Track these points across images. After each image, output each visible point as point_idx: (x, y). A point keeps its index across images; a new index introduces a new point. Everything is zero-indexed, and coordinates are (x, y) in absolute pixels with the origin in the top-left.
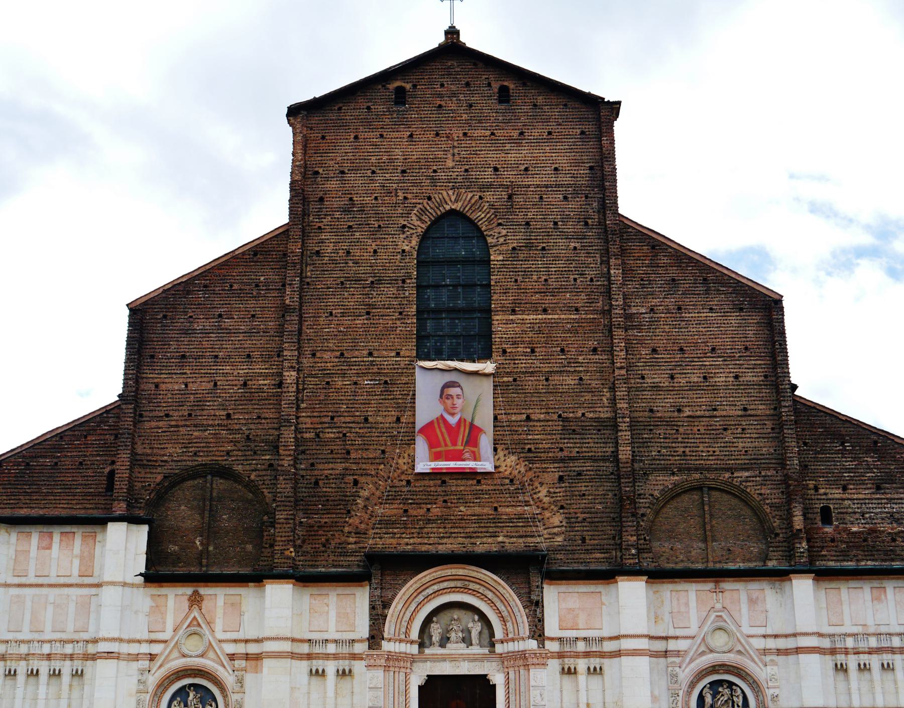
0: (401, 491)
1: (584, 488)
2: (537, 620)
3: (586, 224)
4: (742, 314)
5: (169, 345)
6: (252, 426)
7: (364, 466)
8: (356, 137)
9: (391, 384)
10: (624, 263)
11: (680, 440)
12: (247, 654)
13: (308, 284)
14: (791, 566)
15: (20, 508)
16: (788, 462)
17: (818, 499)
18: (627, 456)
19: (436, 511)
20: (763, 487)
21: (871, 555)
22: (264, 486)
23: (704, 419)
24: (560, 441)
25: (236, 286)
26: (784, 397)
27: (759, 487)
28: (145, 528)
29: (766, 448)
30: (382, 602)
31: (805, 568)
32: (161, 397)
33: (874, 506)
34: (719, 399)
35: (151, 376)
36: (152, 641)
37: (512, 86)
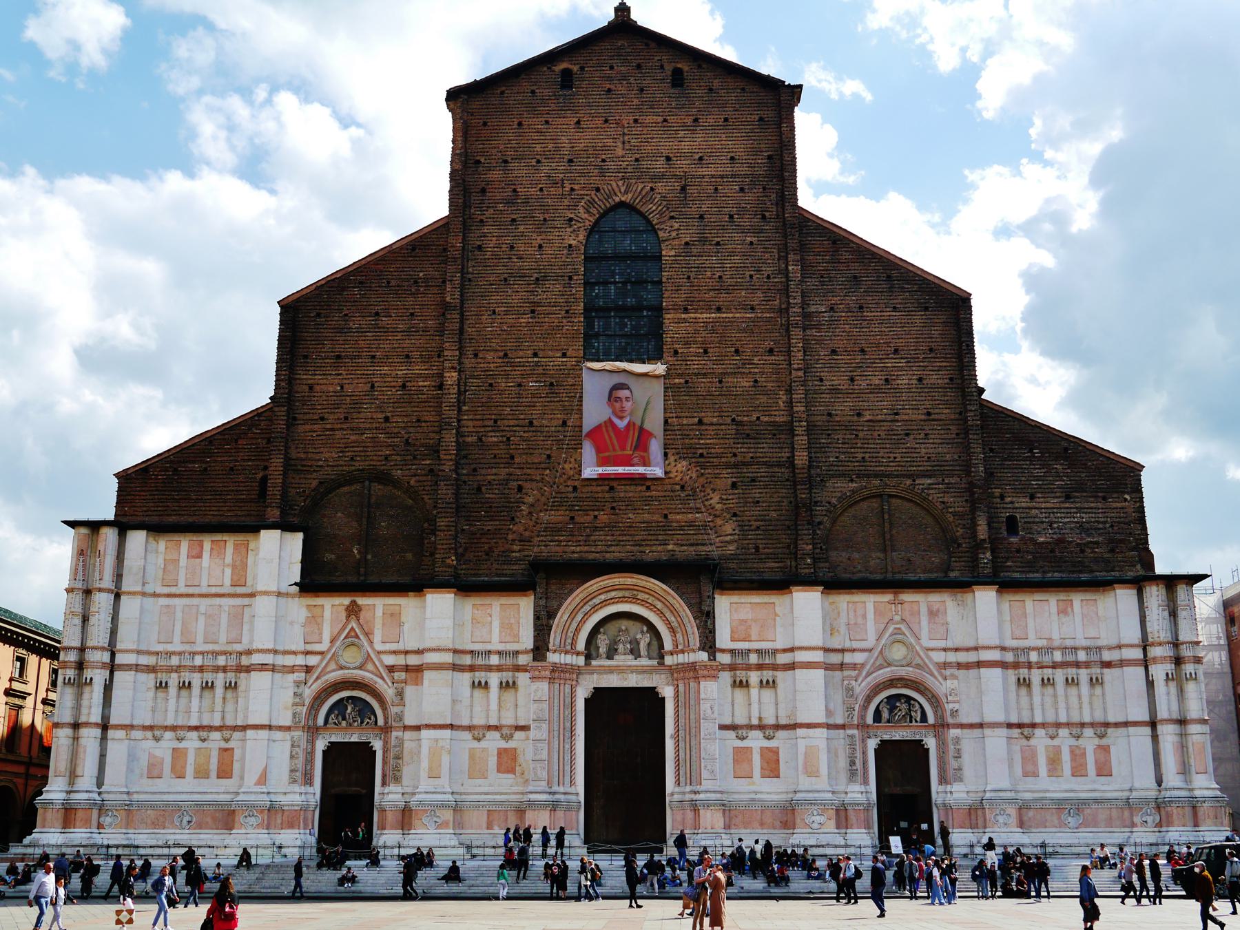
0: (567, 498)
1: (757, 495)
3: (764, 217)
4: (927, 313)
5: (323, 344)
6: (411, 430)
7: (529, 471)
8: (520, 124)
9: (557, 385)
10: (802, 259)
11: (859, 445)
12: (407, 666)
13: (470, 280)
14: (974, 577)
15: (168, 515)
16: (973, 469)
17: (1003, 508)
18: (803, 462)
19: (603, 517)
21: (1058, 567)
22: (424, 492)
23: (885, 423)
24: (734, 446)
25: (393, 283)
26: (970, 400)
27: (942, 495)
28: (300, 536)
29: (950, 454)
30: (547, 612)
31: (989, 580)
32: (315, 399)
33: (1063, 515)
34: (902, 403)
35: (305, 377)
36: (307, 653)
37: (686, 68)
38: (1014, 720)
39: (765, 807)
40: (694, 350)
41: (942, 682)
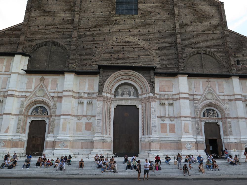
2: (153, 87)
6: (65, 31)
7: (99, 43)
11: (194, 39)
12: (58, 96)
20: (220, 53)
28: (28, 58)
29: (220, 42)
32: (37, 22)
34: (206, 29)
35: (34, 16)
39: (171, 143)
40: (147, 13)
41: (224, 105)
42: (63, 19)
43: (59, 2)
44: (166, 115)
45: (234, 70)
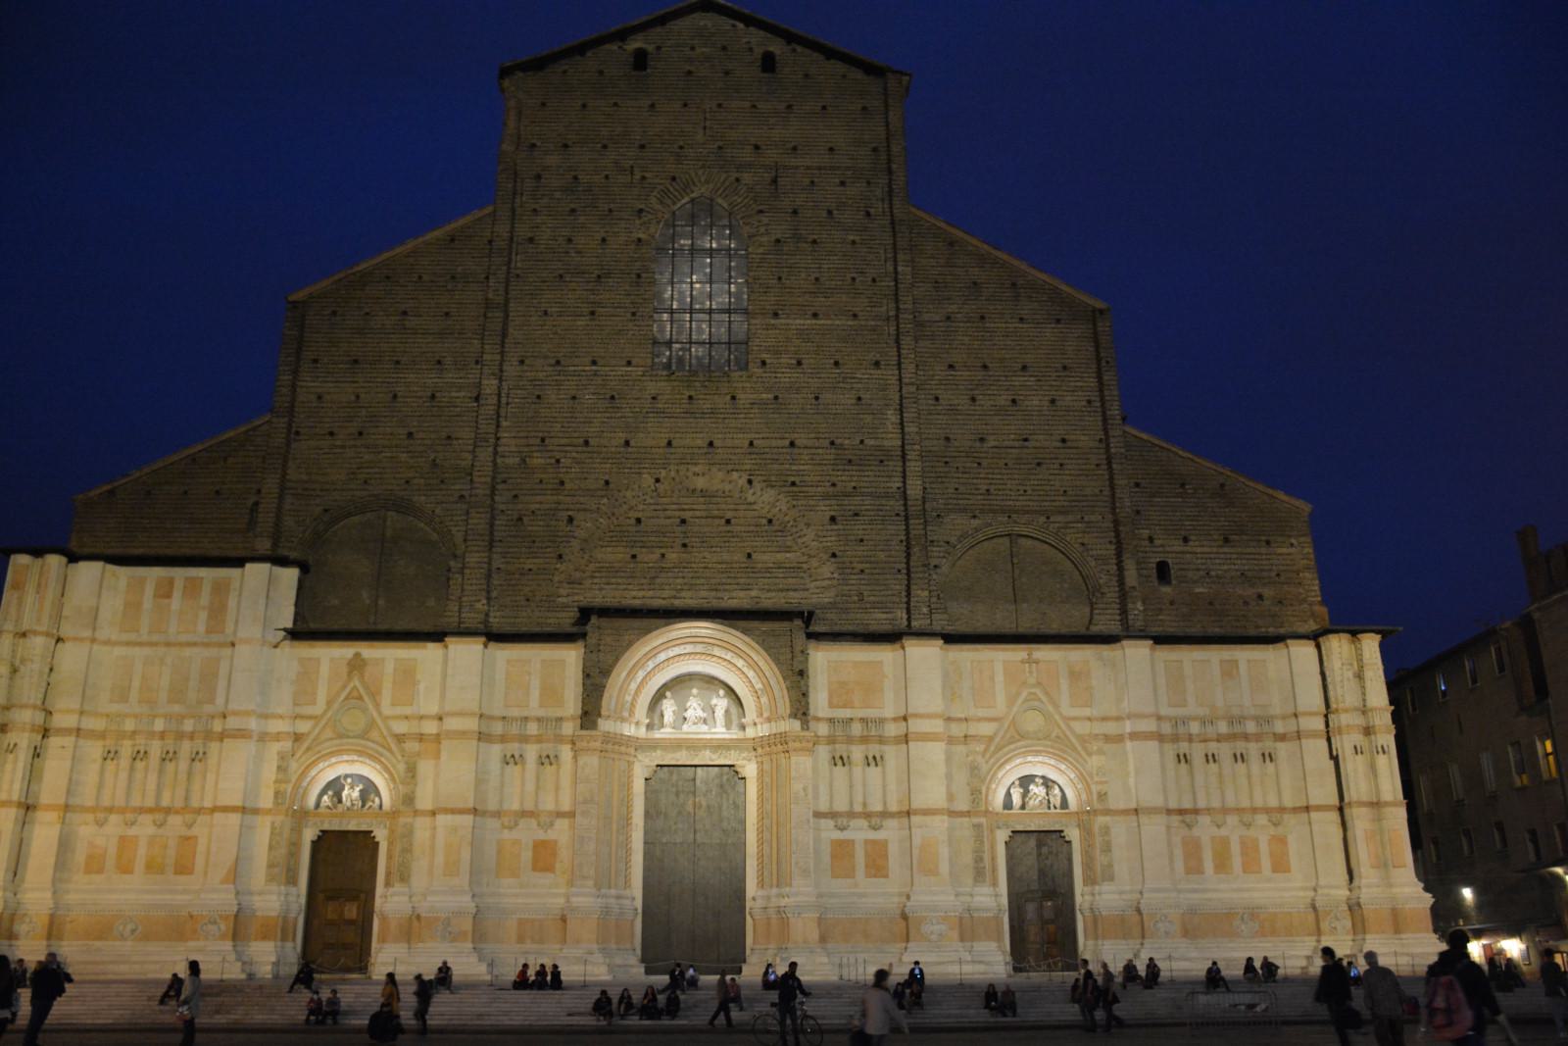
0: (628, 532)
3: (868, 214)
4: (1059, 326)
7: (582, 499)
9: (619, 399)
11: (981, 476)
12: (422, 735)
18: (917, 492)
20: (1086, 535)
22: (452, 523)
23: (1013, 451)
24: (832, 473)
25: (425, 278)
34: (1032, 427)
38: (1173, 804)
42: (433, 397)
43: (412, 318)
44: (851, 804)
45: (1136, 612)
